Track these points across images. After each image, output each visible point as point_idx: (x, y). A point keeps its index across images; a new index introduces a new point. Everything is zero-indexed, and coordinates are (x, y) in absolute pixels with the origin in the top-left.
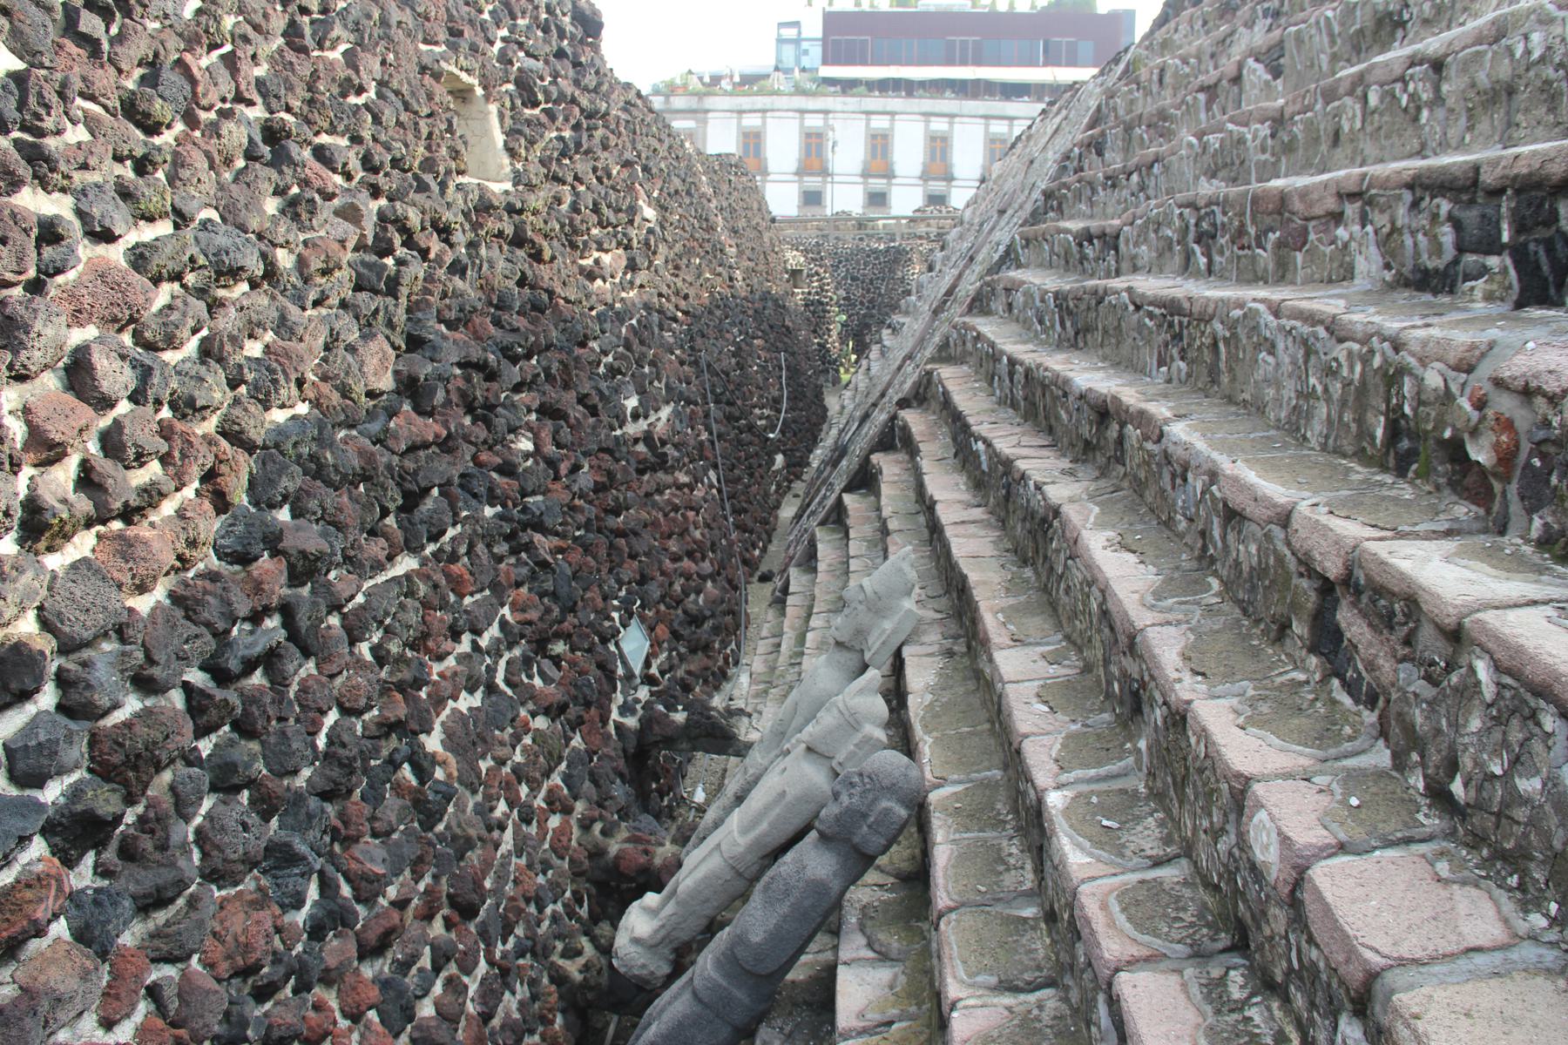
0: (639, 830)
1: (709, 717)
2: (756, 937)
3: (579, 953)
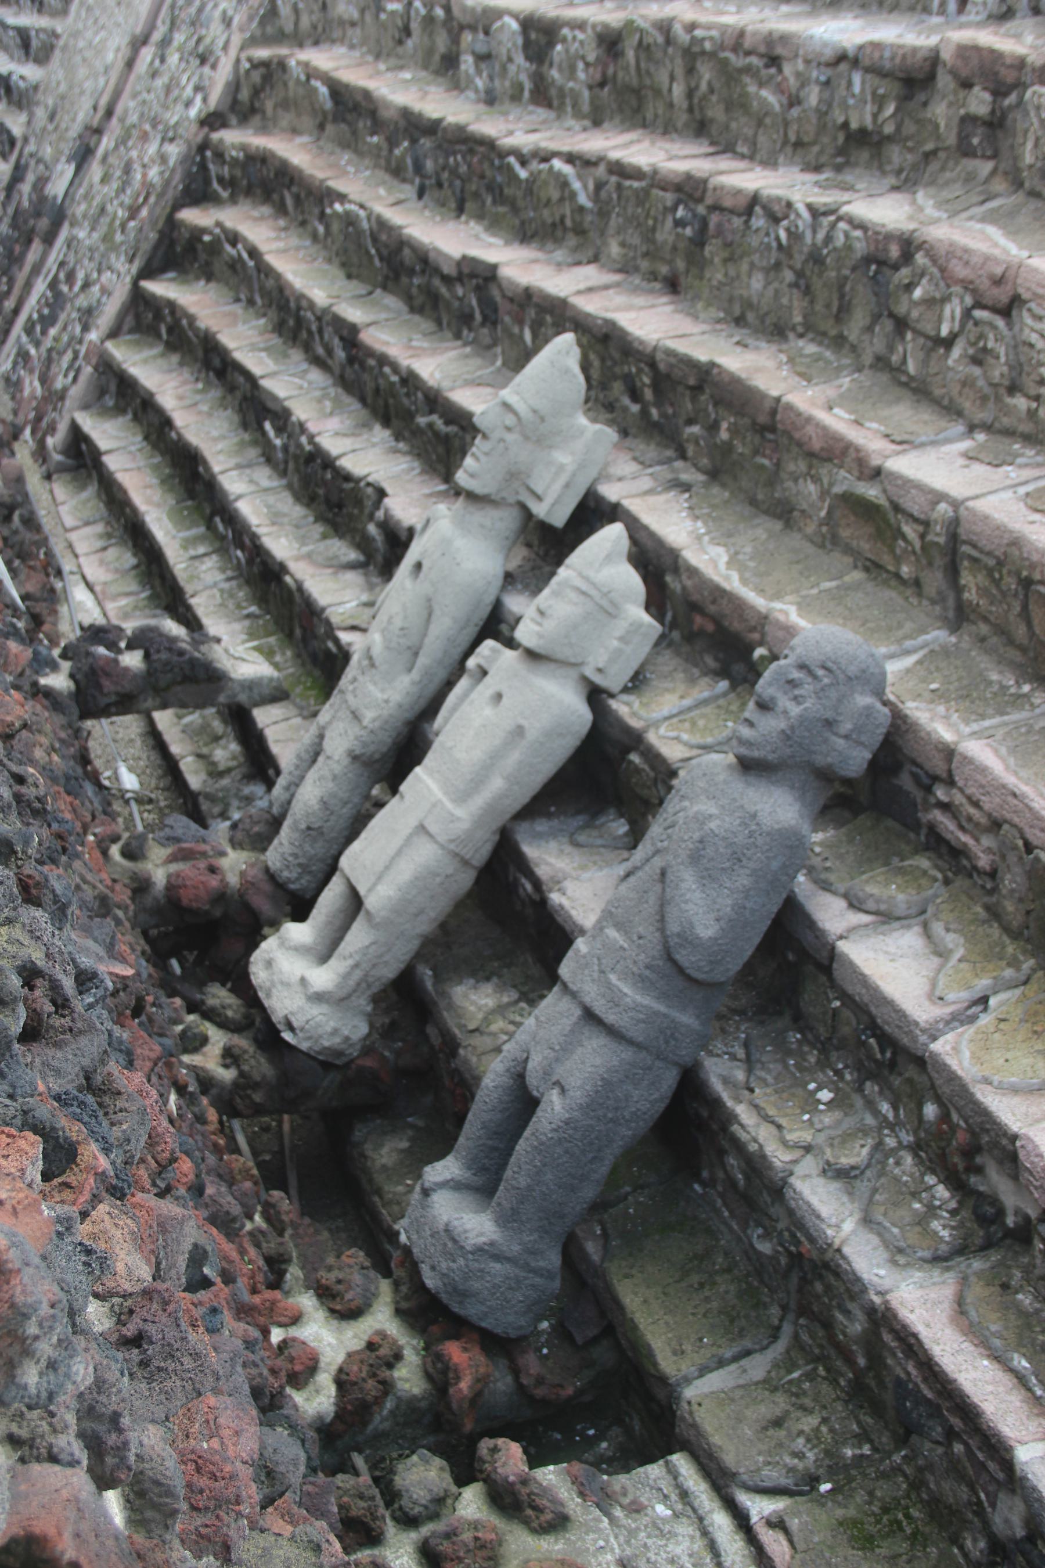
0: (177, 840)
1: (181, 653)
2: (706, 929)
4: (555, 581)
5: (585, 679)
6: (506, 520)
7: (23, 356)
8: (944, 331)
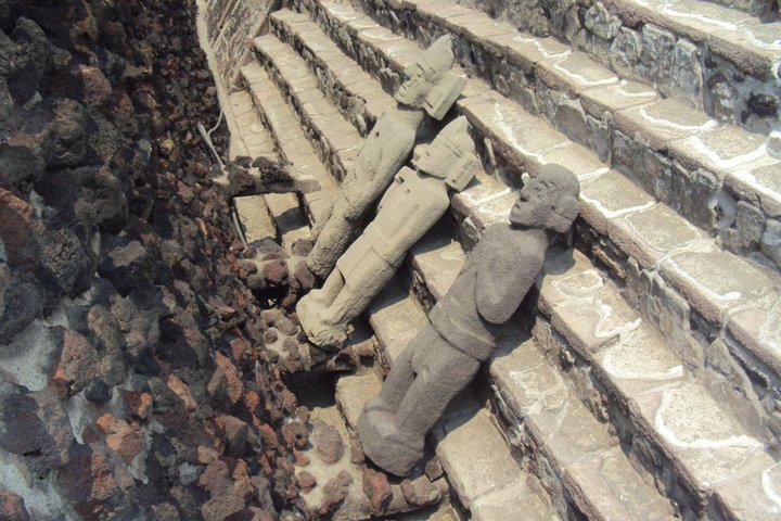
1: (275, 169)
2: (495, 300)
3: (275, 339)
4: (435, 140)
5: (447, 184)
6: (418, 115)
7: (224, 45)
8: (609, 37)
